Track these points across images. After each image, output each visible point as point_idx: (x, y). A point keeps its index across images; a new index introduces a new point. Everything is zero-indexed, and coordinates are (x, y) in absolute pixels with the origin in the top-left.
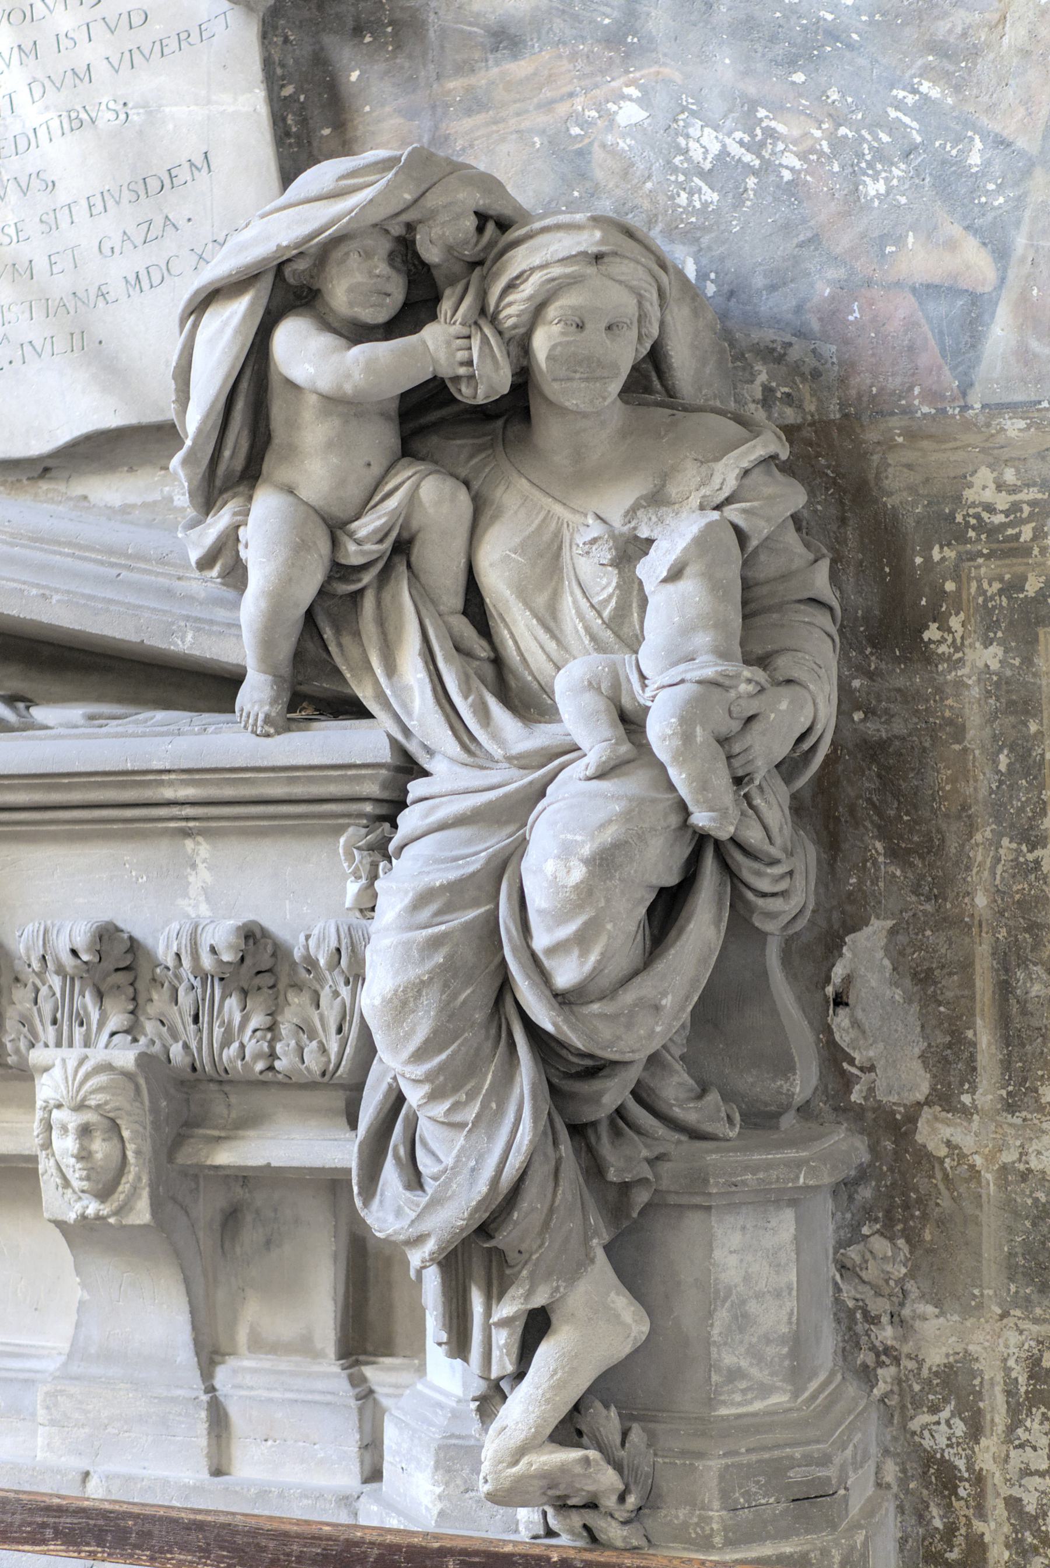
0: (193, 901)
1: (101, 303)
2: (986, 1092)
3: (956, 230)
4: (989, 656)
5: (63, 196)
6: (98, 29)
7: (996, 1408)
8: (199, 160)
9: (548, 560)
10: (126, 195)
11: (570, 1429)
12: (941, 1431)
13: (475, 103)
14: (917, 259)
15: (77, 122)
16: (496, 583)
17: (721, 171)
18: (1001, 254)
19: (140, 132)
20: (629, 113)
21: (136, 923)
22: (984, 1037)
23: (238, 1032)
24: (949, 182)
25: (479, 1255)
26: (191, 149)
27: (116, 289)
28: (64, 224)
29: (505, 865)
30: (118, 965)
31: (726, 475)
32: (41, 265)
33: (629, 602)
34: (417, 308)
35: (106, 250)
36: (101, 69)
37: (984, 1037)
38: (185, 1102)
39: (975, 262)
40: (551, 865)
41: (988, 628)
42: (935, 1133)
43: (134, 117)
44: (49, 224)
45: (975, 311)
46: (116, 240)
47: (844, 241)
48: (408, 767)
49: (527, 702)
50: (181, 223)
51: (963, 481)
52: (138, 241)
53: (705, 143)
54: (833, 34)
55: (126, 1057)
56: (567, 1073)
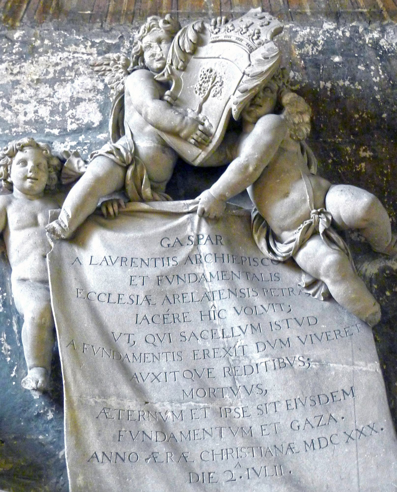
1: (290, 453)
5: (271, 399)
6: (293, 323)
8: (348, 390)
10: (309, 402)
15: (283, 365)
19: (317, 374)
26: (344, 384)
27: (299, 446)
28: (271, 411)
32: (256, 429)
35: (295, 426)
36: (295, 342)
43: (313, 365)
44: (262, 411)
46: (302, 422)
50: (339, 419)
52: (315, 425)
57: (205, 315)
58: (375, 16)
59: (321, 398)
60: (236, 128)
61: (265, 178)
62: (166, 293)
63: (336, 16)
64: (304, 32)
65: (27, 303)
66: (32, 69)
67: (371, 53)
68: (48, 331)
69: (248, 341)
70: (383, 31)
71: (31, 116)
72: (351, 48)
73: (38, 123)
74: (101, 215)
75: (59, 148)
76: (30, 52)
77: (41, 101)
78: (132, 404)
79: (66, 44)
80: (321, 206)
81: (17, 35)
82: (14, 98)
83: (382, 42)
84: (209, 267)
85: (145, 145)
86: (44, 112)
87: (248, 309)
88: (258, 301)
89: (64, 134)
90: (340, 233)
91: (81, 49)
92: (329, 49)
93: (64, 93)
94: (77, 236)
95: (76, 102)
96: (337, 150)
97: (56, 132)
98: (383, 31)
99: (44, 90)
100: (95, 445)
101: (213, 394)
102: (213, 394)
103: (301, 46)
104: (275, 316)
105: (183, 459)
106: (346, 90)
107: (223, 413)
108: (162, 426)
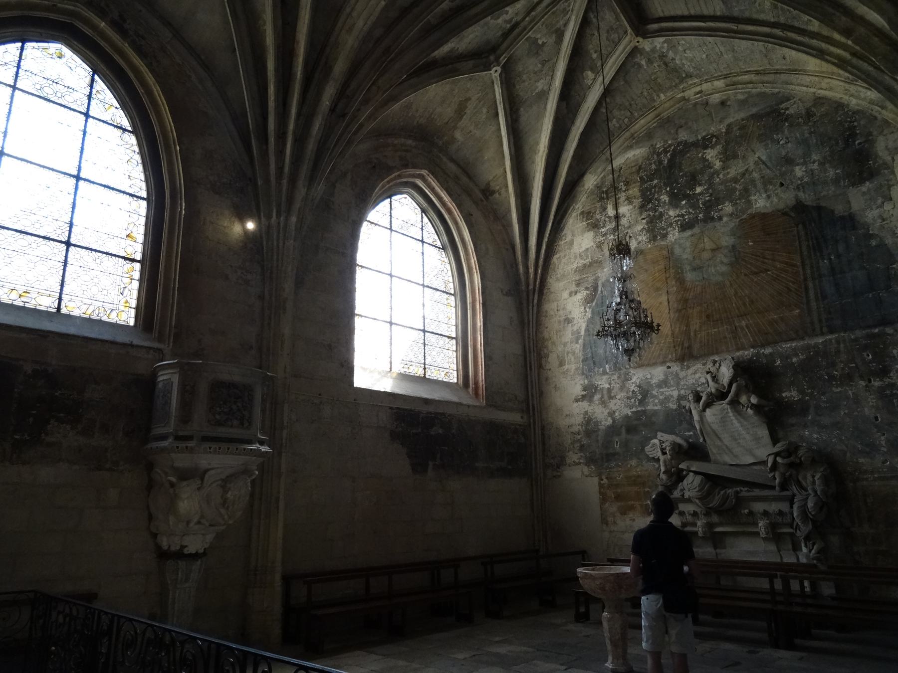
9: (805, 478)
11: (818, 552)
16: (800, 478)
17: (817, 438)
25: (807, 538)
31: (822, 469)
33: (814, 480)
34: (789, 456)
49: (806, 490)
53: (815, 436)
56: (814, 522)
57: (732, 424)
58: (763, 346)
59: (757, 439)
60: (730, 385)
61: (737, 395)
62: (723, 420)
63: (753, 347)
64: (746, 353)
65: (698, 427)
66: (690, 371)
68: (701, 431)
69: (740, 429)
72: (758, 355)
73: (693, 384)
74: (708, 405)
75: (699, 389)
76: (688, 368)
78: (720, 444)
80: (749, 401)
84: (731, 414)
85: (713, 390)
87: (740, 422)
88: (742, 420)
90: (753, 406)
92: (753, 356)
93: (697, 376)
94: (704, 410)
100: (714, 451)
101: (736, 440)
102: (736, 440)
104: (745, 423)
105: (732, 453)
107: (739, 443)
108: (727, 447)
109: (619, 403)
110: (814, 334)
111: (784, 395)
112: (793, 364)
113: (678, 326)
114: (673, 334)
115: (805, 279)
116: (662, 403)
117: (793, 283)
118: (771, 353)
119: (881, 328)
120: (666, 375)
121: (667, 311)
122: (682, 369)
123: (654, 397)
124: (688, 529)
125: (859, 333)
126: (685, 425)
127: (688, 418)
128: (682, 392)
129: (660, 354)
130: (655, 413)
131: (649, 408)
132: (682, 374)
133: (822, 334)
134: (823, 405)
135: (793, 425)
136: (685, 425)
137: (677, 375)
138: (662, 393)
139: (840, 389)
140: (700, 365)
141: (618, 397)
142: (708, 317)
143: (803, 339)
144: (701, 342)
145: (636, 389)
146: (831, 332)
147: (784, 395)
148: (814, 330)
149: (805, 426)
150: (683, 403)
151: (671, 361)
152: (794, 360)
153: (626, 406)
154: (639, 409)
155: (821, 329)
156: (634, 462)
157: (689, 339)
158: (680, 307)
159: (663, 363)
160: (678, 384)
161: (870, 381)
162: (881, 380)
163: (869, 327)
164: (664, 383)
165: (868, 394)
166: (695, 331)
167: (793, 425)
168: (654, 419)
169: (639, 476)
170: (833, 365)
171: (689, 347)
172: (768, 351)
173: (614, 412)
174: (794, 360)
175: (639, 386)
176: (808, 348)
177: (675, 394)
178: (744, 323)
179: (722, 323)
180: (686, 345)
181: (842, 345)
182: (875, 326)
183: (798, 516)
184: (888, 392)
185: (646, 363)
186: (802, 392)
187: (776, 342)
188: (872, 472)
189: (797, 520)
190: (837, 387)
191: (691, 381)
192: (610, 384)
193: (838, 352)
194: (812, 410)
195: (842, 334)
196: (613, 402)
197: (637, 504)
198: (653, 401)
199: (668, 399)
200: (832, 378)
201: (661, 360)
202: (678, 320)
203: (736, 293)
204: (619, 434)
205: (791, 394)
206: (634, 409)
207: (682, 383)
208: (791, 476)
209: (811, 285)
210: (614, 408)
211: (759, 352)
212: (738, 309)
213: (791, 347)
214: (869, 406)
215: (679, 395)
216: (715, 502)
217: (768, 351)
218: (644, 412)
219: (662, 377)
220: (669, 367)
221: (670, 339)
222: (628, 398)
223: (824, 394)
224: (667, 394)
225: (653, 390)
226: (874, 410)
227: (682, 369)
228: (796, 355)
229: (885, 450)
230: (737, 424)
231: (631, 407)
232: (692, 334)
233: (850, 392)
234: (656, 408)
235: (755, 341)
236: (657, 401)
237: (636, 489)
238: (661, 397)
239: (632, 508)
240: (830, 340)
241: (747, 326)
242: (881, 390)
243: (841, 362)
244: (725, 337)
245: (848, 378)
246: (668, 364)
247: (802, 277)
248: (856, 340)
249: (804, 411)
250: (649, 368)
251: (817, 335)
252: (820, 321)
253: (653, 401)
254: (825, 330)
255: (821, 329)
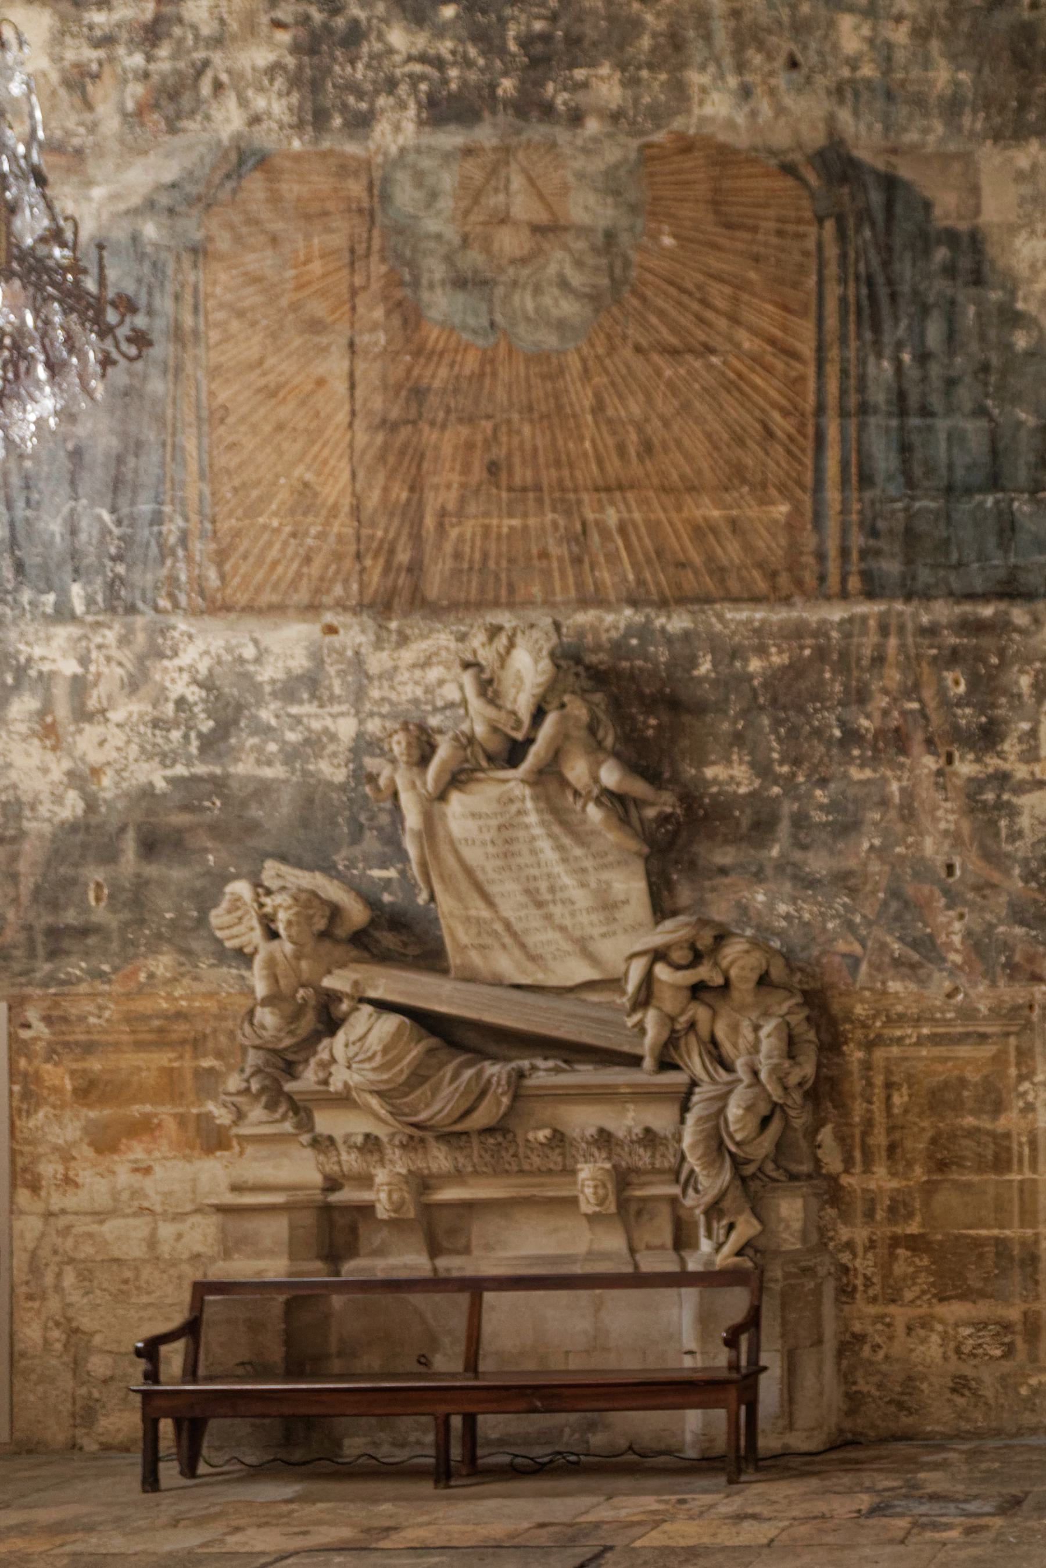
0: (627, 1121)
2: (858, 1169)
3: (851, 938)
4: (860, 1054)
7: (860, 1250)
12: (845, 1258)
13: (714, 889)
14: (841, 946)
17: (787, 917)
18: (864, 946)
20: (761, 898)
21: (611, 1126)
22: (858, 1155)
23: (643, 1158)
24: (850, 926)
29: (722, 1111)
30: (604, 1139)
33: (758, 1037)
37: (858, 1155)
38: (623, 1179)
39: (857, 948)
40: (734, 1111)
41: (860, 1045)
42: (845, 1180)
45: (855, 962)
47: (822, 939)
48: (694, 1083)
51: (853, 1007)
53: (783, 908)
54: (819, 881)
55: (608, 1166)
58: (663, 604)
63: (634, 603)
64: (609, 618)
66: (408, 655)
67: (658, 635)
70: (669, 617)
71: (410, 696)
72: (644, 632)
73: (416, 702)
76: (404, 640)
77: (417, 683)
79: (431, 631)
81: (393, 625)
82: (397, 680)
83: (669, 628)
86: (419, 692)
89: (436, 710)
91: (443, 636)
93: (434, 674)
95: (441, 683)
96: (633, 718)
97: (429, 708)
98: (669, 617)
99: (418, 673)
103: (607, 631)
106: (640, 669)
109: (118, 738)
110: (822, 594)
111: (709, 772)
112: (750, 677)
113: (381, 478)
114: (356, 510)
115: (820, 409)
116: (291, 755)
117: (785, 413)
118: (687, 636)
119: (1003, 606)
120: (317, 657)
121: (342, 416)
122: (378, 644)
123: (266, 731)
124: (348, 1195)
125: (942, 611)
126: (371, 843)
127: (384, 819)
128: (373, 726)
129: (299, 575)
130: (263, 790)
131: (240, 769)
132: (377, 662)
133: (844, 595)
134: (818, 817)
135: (723, 871)
136: (371, 843)
137: (358, 661)
138: (298, 720)
139: (867, 774)
140: (443, 639)
141: (117, 716)
142: (493, 468)
143: (787, 600)
144: (457, 556)
145: (194, 693)
146: (870, 595)
147: (709, 772)
148: (822, 578)
149: (758, 876)
150: (371, 763)
151: (340, 605)
152: (755, 665)
153: (146, 754)
154: (201, 769)
155: (844, 580)
156: (163, 964)
157: (417, 538)
158: (395, 414)
159: (312, 609)
160: (359, 695)
161: (950, 760)
162: (978, 760)
163: (971, 597)
164: (307, 684)
165: (940, 796)
166: (443, 513)
167: (723, 871)
168: (255, 812)
169: (180, 1015)
170: (861, 697)
171: (415, 568)
172: (678, 622)
173: (96, 772)
174: (755, 665)
175: (207, 685)
176: (798, 632)
177: (346, 728)
178: (612, 517)
179: (540, 501)
180: (403, 557)
181: (893, 642)
182: (985, 597)
183: (693, 1146)
184: (990, 796)
185: (242, 599)
186: (763, 770)
187: (708, 600)
188: (917, 1021)
189: (693, 1161)
190: (862, 766)
191: (408, 691)
192: (84, 661)
193: (879, 660)
194: (784, 828)
195: (899, 606)
196: (92, 732)
197: (165, 1113)
198: (259, 749)
199: (315, 743)
200: (852, 736)
201: (302, 596)
202: (382, 457)
203: (599, 408)
204: (109, 855)
205: (729, 775)
206: (180, 770)
207: (375, 693)
208: (692, 1025)
209: (832, 432)
210: (95, 757)
211: (649, 621)
212: (600, 462)
213: (750, 621)
214: (938, 835)
215: (360, 735)
216: (436, 1107)
217: (678, 622)
218: (219, 784)
219: (300, 663)
220: (331, 630)
221: (342, 526)
222: (156, 724)
223: (823, 782)
224: (316, 725)
225: (260, 703)
226: (947, 843)
227: (378, 644)
228: (762, 651)
229: (957, 958)
230: (549, 853)
231: (166, 759)
232: (429, 522)
233: (895, 787)
234: (268, 773)
235: (641, 582)
236: (272, 747)
237: (164, 1058)
238: (291, 737)
239: (143, 1128)
240: (864, 619)
241: (622, 529)
242: (976, 785)
243: (885, 691)
244: (544, 555)
245: (897, 741)
246: (329, 617)
247: (811, 399)
248: (931, 631)
249: (762, 827)
250: (251, 623)
251: (828, 598)
252: (844, 552)
253: (259, 749)
254: (854, 583)
255: (844, 580)
